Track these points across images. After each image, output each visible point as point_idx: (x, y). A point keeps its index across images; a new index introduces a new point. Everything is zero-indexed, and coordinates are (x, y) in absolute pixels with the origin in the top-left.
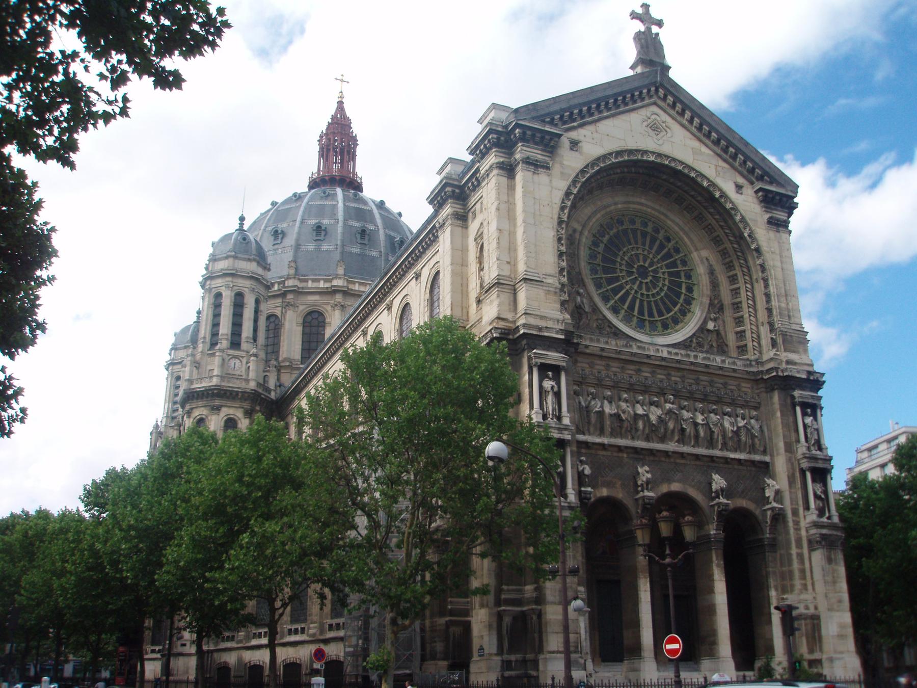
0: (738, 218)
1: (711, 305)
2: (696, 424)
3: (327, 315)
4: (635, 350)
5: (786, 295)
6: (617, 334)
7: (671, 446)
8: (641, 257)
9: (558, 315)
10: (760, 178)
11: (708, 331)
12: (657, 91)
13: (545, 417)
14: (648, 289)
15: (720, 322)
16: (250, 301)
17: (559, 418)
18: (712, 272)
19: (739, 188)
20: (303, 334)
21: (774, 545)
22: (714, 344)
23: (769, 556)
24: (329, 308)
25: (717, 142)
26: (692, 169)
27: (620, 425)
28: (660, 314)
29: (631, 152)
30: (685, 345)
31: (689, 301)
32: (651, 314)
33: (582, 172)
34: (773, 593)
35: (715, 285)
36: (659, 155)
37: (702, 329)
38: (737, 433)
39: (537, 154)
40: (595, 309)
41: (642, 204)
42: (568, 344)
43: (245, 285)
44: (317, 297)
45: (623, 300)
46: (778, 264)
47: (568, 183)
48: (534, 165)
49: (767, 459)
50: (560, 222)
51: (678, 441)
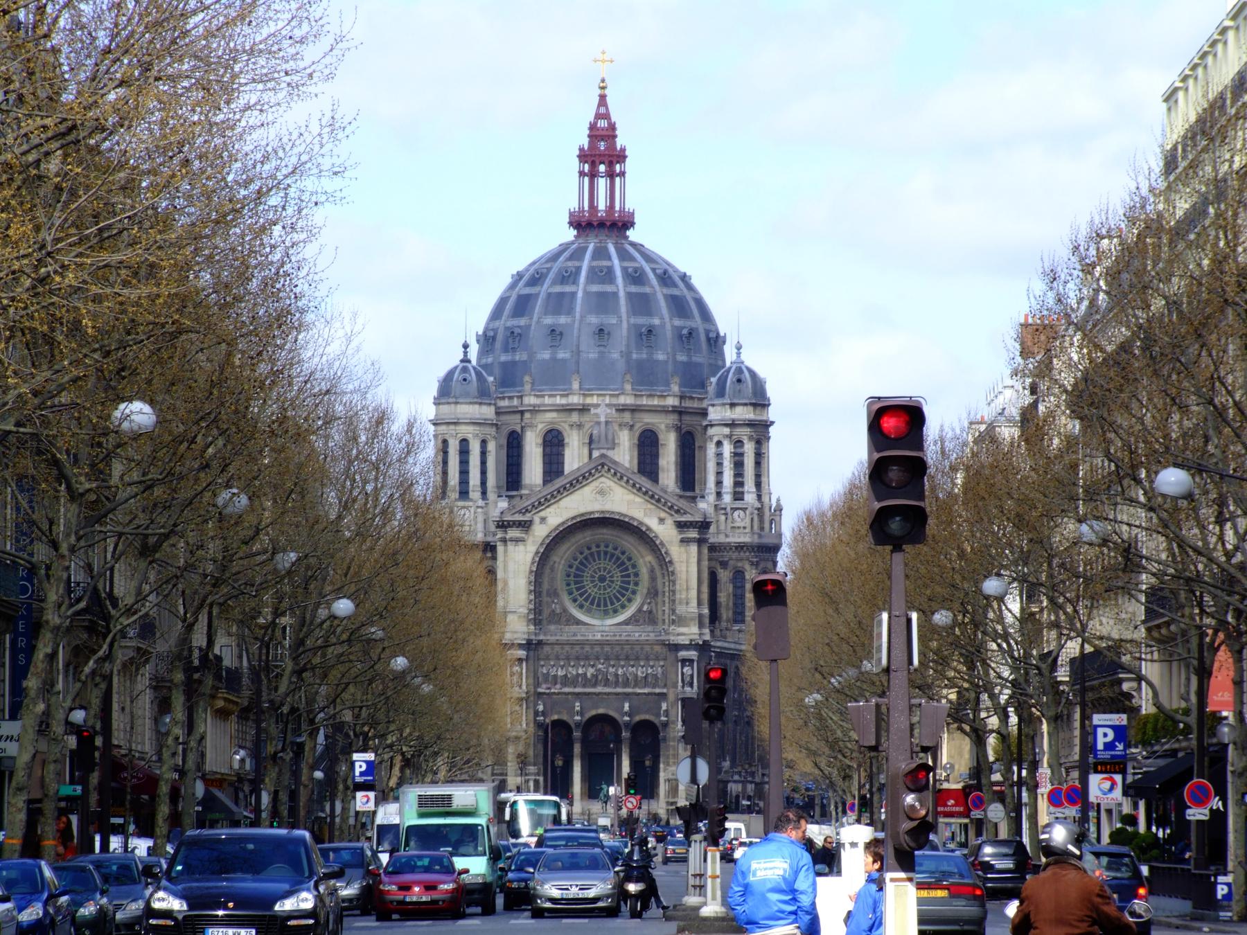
1: (649, 593)
2: (616, 675)
3: (565, 435)
4: (579, 638)
5: (687, 589)
6: (578, 622)
7: (599, 689)
9: (525, 629)
10: (678, 512)
16: (475, 448)
17: (520, 686)
18: (652, 571)
19: (662, 520)
20: (544, 455)
21: (665, 739)
23: (662, 746)
24: (567, 427)
25: (645, 493)
26: (626, 516)
27: (566, 681)
28: (612, 604)
29: (582, 515)
30: (626, 623)
31: (634, 592)
32: (606, 605)
33: (548, 536)
34: (662, 766)
35: (653, 579)
36: (603, 512)
37: (640, 610)
38: (646, 678)
40: (565, 610)
42: (529, 645)
43: (467, 431)
44: (554, 415)
45: (586, 600)
46: (684, 569)
48: (517, 541)
50: (531, 572)
51: (605, 686)
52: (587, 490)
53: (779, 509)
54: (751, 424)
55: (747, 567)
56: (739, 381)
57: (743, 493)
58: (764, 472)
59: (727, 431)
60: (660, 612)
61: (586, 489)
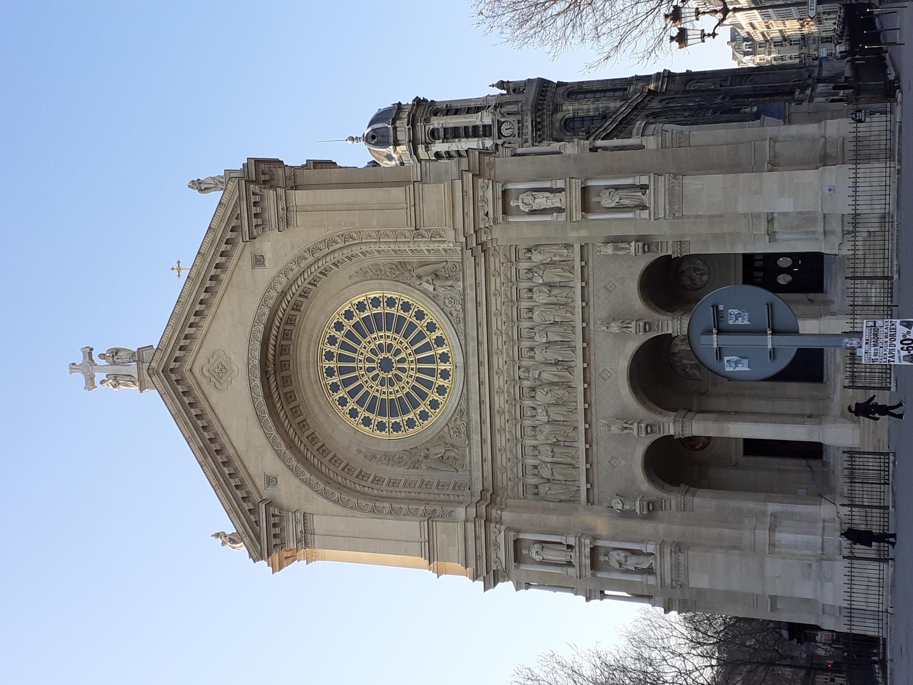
0: (296, 269)
8: (368, 365)
11: (434, 289)
12: (172, 370)
13: (570, 564)
14: (402, 361)
15: (421, 271)
17: (570, 547)
22: (450, 283)
30: (458, 322)
39: (291, 530)
40: (440, 438)
41: (308, 362)
47: (315, 495)
49: (577, 248)
52: (215, 398)
53: (501, 85)
54: (412, 123)
55: (559, 116)
56: (373, 137)
57: (484, 126)
58: (466, 105)
59: (421, 149)
60: (432, 258)
61: (213, 400)
